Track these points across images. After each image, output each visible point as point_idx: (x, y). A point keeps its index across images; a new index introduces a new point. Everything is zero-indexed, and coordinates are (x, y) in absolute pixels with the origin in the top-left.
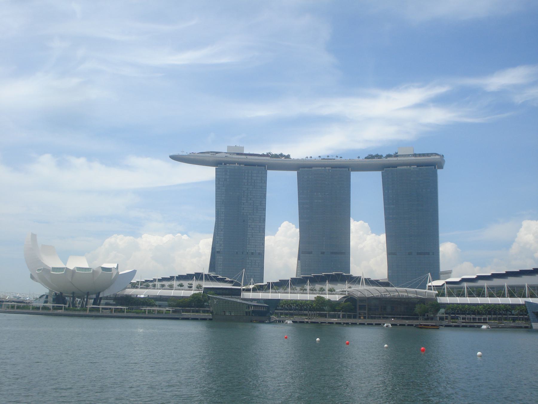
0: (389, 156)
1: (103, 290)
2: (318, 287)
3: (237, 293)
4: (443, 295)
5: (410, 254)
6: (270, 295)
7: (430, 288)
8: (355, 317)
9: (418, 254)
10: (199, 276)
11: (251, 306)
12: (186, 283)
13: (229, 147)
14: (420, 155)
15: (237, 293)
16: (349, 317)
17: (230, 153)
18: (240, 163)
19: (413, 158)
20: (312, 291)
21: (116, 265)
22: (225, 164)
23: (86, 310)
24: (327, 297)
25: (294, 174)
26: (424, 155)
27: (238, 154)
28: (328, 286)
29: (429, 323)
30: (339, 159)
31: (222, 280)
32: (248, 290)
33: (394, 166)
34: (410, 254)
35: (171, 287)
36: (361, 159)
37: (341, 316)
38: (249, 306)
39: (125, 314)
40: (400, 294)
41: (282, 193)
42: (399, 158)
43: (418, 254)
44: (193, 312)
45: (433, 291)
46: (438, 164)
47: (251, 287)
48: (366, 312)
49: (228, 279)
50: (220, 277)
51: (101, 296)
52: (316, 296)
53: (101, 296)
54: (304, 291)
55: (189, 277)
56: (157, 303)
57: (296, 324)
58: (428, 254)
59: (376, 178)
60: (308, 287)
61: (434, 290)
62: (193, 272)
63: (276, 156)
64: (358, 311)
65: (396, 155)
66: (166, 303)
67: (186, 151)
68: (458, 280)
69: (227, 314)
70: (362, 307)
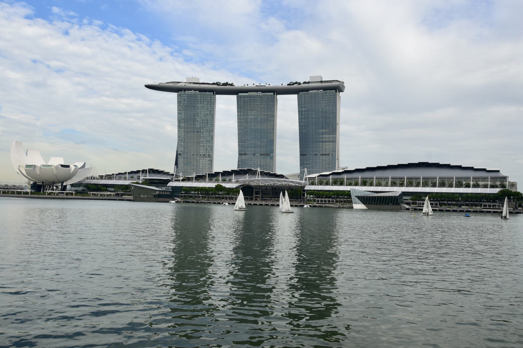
0: (305, 83)
1: (66, 180)
8: (252, 199)
9: (322, 155)
10: (144, 171)
13: (187, 78)
14: (325, 82)
18: (195, 90)
20: (224, 181)
21: (83, 163)
22: (185, 91)
24: (224, 185)
25: (234, 98)
26: (328, 82)
27: (194, 83)
30: (267, 85)
33: (307, 90)
42: (310, 85)
43: (322, 155)
46: (337, 88)
47: (181, 178)
48: (260, 196)
52: (216, 184)
55: (138, 172)
58: (329, 155)
60: (220, 178)
64: (254, 195)
65: (309, 83)
70: (257, 193)
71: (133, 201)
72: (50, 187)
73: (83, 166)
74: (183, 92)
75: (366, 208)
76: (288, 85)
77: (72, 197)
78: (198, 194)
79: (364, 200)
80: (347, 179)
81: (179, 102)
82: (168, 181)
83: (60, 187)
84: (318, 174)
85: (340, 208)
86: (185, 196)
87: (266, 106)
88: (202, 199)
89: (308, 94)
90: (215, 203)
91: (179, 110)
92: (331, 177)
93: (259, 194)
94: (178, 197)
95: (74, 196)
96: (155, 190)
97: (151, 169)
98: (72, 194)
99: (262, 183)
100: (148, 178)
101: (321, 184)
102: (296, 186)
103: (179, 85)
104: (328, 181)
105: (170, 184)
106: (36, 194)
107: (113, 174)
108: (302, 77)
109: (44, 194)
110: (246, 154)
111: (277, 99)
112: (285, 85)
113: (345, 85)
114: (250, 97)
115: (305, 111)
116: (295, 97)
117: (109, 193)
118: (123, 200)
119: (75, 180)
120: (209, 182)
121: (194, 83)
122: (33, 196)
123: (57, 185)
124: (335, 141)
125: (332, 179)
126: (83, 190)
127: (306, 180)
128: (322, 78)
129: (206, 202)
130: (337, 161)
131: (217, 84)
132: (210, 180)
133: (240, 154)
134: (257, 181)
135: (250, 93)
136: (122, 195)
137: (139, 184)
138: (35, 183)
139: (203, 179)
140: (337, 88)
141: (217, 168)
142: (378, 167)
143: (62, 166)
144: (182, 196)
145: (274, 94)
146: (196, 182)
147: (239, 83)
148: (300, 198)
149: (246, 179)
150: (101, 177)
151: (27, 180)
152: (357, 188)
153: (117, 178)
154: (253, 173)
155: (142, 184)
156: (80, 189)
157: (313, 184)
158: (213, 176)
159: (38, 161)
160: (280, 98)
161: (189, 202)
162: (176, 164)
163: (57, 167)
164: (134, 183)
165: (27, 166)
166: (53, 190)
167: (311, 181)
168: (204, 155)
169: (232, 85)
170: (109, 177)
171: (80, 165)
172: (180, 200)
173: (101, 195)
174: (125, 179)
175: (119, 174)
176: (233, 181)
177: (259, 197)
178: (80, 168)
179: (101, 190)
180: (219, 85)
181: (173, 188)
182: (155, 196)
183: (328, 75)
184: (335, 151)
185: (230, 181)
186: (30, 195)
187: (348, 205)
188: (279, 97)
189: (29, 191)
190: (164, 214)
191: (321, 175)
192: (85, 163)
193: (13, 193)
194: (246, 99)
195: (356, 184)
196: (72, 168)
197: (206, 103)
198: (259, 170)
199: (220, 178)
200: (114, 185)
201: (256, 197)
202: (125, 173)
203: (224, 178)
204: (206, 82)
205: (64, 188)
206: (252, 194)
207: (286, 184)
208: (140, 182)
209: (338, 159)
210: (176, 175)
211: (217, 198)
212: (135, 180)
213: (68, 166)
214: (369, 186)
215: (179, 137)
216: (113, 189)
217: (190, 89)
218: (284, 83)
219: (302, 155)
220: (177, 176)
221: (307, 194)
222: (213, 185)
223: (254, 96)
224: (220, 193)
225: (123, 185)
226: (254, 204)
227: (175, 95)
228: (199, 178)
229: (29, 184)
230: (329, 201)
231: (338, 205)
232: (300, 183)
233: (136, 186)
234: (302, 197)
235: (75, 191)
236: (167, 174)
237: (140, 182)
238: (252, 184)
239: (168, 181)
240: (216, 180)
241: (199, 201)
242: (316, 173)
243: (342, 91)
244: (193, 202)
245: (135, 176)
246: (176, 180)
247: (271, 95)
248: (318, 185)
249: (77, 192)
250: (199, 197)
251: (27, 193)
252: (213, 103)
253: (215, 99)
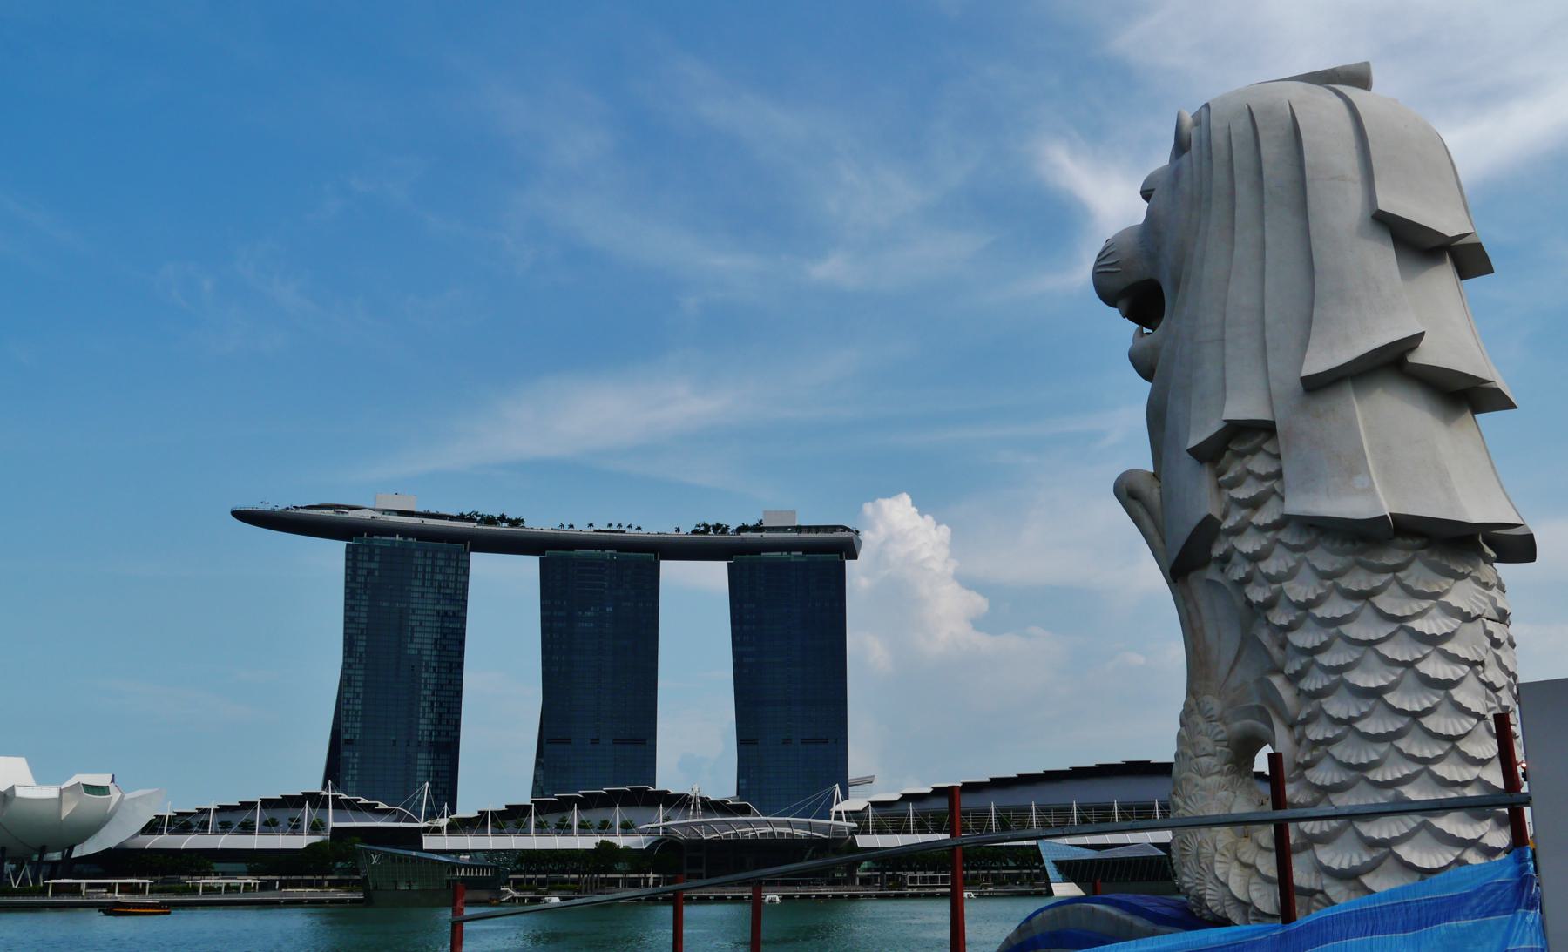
0: (744, 528)
2: (596, 816)
3: (414, 838)
4: (865, 832)
5: (787, 741)
6: (490, 842)
7: (838, 817)
11: (460, 866)
12: (283, 815)
15: (414, 838)
17: (384, 511)
18: (405, 532)
19: (795, 535)
23: (44, 891)
24: (622, 841)
26: (817, 529)
27: (401, 513)
28: (618, 815)
29: (843, 891)
31: (371, 809)
32: (437, 830)
34: (787, 741)
35: (247, 828)
36: (682, 532)
37: (651, 882)
38: (454, 867)
39: (149, 899)
40: (777, 830)
41: (504, 605)
43: (804, 741)
44: (309, 884)
45: (844, 823)
46: (847, 548)
48: (703, 871)
49: (382, 806)
50: (363, 801)
51: (75, 855)
52: (599, 839)
53: (75, 855)
54: (564, 828)
56: (218, 867)
58: (826, 741)
59: (714, 575)
60: (575, 817)
61: (848, 819)
62: (296, 792)
63: (490, 520)
65: (758, 528)
66: (242, 867)
68: (896, 797)
69: (403, 887)
75: (1081, 893)
79: (1070, 870)
103: (352, 514)
110: (568, 741)
112: (687, 529)
121: (401, 513)
135: (578, 552)
160: (670, 570)
169: (516, 523)
172: (517, 895)
183: (808, 509)
197: (440, 577)
204: (433, 511)
207: (780, 834)
217: (390, 530)
222: (588, 842)
227: (338, 548)
233: (386, 855)
243: (855, 557)
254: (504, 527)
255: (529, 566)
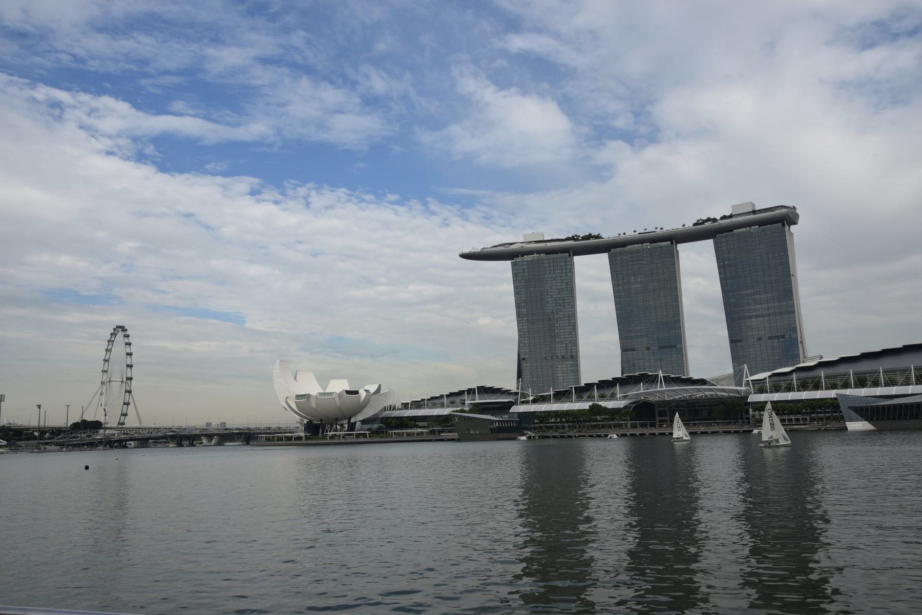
1: (355, 414)
7: (747, 384)
8: (653, 425)
9: (771, 338)
10: (470, 391)
14: (761, 211)
16: (642, 426)
18: (539, 252)
20: (602, 397)
22: (522, 256)
24: (603, 404)
26: (766, 210)
30: (659, 230)
33: (729, 229)
37: (629, 426)
42: (733, 220)
43: (771, 338)
46: (787, 218)
47: (531, 398)
52: (590, 403)
55: (461, 393)
56: (420, 424)
57: (624, 439)
60: (596, 393)
64: (658, 418)
67: (476, 246)
70: (662, 414)
71: (459, 440)
72: (331, 426)
73: (378, 391)
74: (519, 259)
76: (694, 225)
77: (365, 440)
78: (561, 422)
80: (826, 377)
81: (515, 275)
82: (511, 404)
83: (346, 426)
84: (769, 373)
85: (819, 430)
86: (541, 428)
87: (660, 265)
88: (569, 431)
89: (732, 235)
90: (591, 436)
91: (516, 288)
92: (794, 376)
93: (666, 415)
94: (529, 430)
95: (368, 439)
96: (493, 421)
97: (482, 387)
98: (365, 435)
99: (669, 396)
100: (477, 401)
101: (777, 391)
102: (731, 397)
103: (512, 247)
104: (790, 384)
105: (515, 409)
106: (313, 439)
107: (423, 400)
108: (718, 210)
109: (325, 437)
110: (634, 350)
111: (677, 252)
112: (689, 224)
113: (798, 211)
114: (631, 252)
115: (730, 265)
116: (710, 243)
117: (420, 430)
118: (443, 440)
119: (368, 413)
120: (578, 401)
122: (309, 442)
123: (342, 422)
124: (793, 312)
125: (798, 379)
126: (379, 428)
127: (747, 384)
128: (753, 205)
129: (577, 435)
130: (800, 345)
131: (573, 238)
132: (580, 398)
133: (624, 350)
134: (660, 392)
135: (629, 247)
136: (440, 432)
137: (465, 412)
138: (311, 421)
139: (568, 397)
140: (787, 218)
141: (587, 376)
142: (884, 350)
143: (348, 392)
144: (535, 428)
145: (672, 243)
146: (556, 402)
147: (609, 234)
148: (742, 419)
149: (641, 390)
150: (405, 406)
151: (298, 418)
152: (848, 392)
153: (430, 405)
154: (652, 380)
155: (470, 412)
156: (375, 426)
157: (761, 391)
158: (584, 391)
159: (314, 389)
161: (548, 437)
162: (520, 375)
163: (340, 395)
164: (457, 411)
165: (298, 397)
166: (336, 430)
167: (757, 387)
168: (563, 357)
169: (598, 237)
170: (418, 404)
171: (373, 388)
173: (408, 434)
174: (442, 406)
175: (432, 398)
176: (618, 396)
177: (666, 421)
178: (374, 394)
179: (407, 427)
180: (577, 240)
181: (521, 415)
182: (492, 430)
184: (794, 329)
185: (613, 397)
186: (304, 441)
187: (834, 425)
188: (681, 247)
189: (302, 434)
190: (507, 460)
191: (774, 375)
192: (380, 386)
193: (280, 439)
194: (624, 258)
195: (846, 386)
196: (363, 394)
197: (558, 271)
198: (661, 374)
199: (596, 393)
200: (426, 416)
201: (660, 421)
202: (442, 396)
203: (602, 392)
205: (352, 427)
206: (653, 417)
208: (467, 409)
209: (802, 342)
210: (523, 394)
211: (594, 427)
212: (458, 406)
213: (356, 392)
214: (870, 387)
215: (520, 331)
216: (425, 424)
218: (688, 222)
219: (734, 341)
220: (524, 395)
221: (754, 410)
222: (585, 405)
223: (637, 251)
224: (599, 418)
225: (439, 416)
226: (660, 434)
228: (560, 396)
229: (301, 423)
230: (797, 420)
231: (815, 425)
232: (737, 391)
234: (745, 416)
235: (369, 430)
236: (507, 392)
237: (467, 409)
238: (651, 399)
239: (511, 404)
240: (589, 397)
241: (565, 435)
242: (764, 371)
243: (796, 224)
244: (556, 437)
245: (458, 400)
246: (523, 402)
247: (667, 246)
248: (771, 392)
249: (374, 433)
250: (564, 428)
251: (300, 438)
252: (569, 271)
253: (572, 264)
254: (592, 241)
255: (603, 259)
